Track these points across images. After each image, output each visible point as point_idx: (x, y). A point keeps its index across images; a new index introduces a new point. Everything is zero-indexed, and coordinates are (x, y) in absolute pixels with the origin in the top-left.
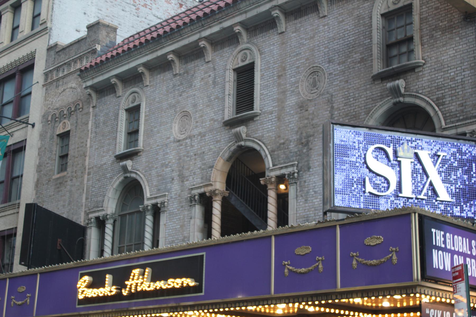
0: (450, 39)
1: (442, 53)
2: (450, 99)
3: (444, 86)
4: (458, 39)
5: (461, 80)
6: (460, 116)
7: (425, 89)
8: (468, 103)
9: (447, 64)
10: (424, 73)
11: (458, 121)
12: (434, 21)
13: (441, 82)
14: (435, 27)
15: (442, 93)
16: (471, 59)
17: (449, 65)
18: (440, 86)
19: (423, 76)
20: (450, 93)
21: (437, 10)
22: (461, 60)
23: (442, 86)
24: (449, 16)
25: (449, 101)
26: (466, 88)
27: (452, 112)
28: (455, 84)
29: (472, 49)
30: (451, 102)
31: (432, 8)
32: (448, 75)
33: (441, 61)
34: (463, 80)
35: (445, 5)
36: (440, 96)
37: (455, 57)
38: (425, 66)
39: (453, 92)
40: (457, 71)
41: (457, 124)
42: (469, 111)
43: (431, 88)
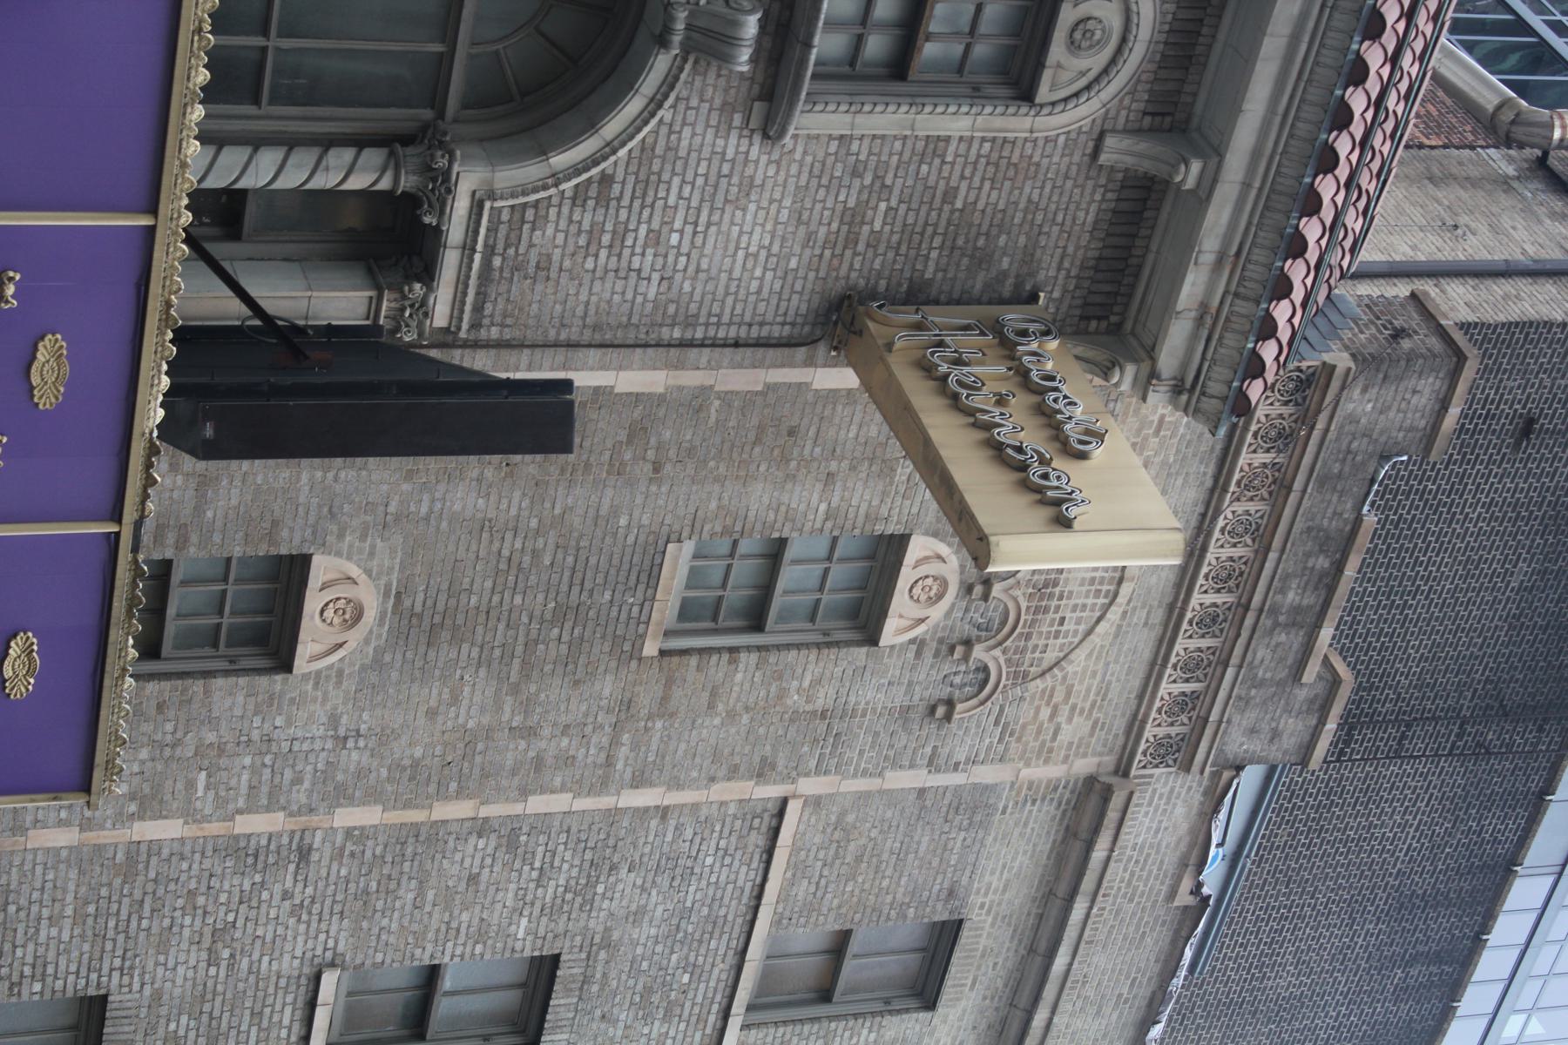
0: (810, 236)
1: (774, 207)
2: (586, 226)
3: (643, 207)
4: (793, 263)
5: (636, 265)
6: (504, 259)
7: (671, 132)
8: (539, 287)
9: (719, 224)
10: (734, 134)
11: (490, 251)
12: (910, 182)
13: (666, 199)
14: (883, 186)
15: (619, 199)
16: (693, 306)
17: (713, 229)
18: (651, 193)
19: (723, 127)
20: (609, 227)
21: (945, 193)
22: (708, 271)
23: (649, 200)
24: (895, 238)
25: (580, 223)
26: (598, 284)
27: (533, 230)
28: (633, 246)
29: (728, 311)
30: (573, 229)
31: (962, 177)
32: (677, 225)
33: (743, 201)
34: (634, 274)
35: (943, 223)
36: (616, 188)
37: (731, 251)
38: (757, 138)
39: (606, 239)
40: (679, 254)
41: (477, 257)
42: (509, 291)
43: (663, 158)
